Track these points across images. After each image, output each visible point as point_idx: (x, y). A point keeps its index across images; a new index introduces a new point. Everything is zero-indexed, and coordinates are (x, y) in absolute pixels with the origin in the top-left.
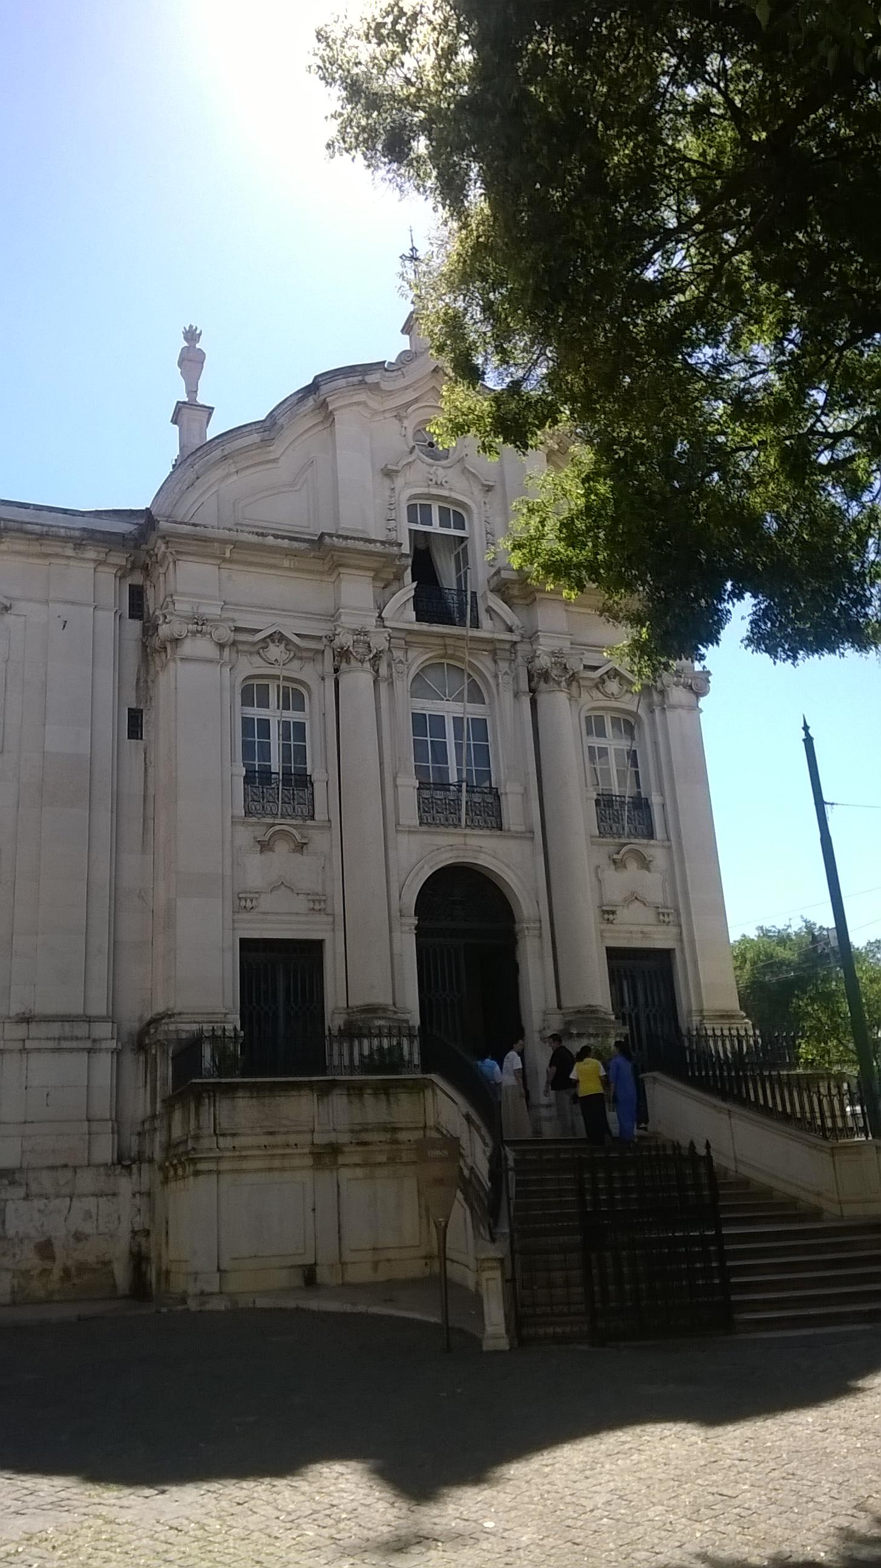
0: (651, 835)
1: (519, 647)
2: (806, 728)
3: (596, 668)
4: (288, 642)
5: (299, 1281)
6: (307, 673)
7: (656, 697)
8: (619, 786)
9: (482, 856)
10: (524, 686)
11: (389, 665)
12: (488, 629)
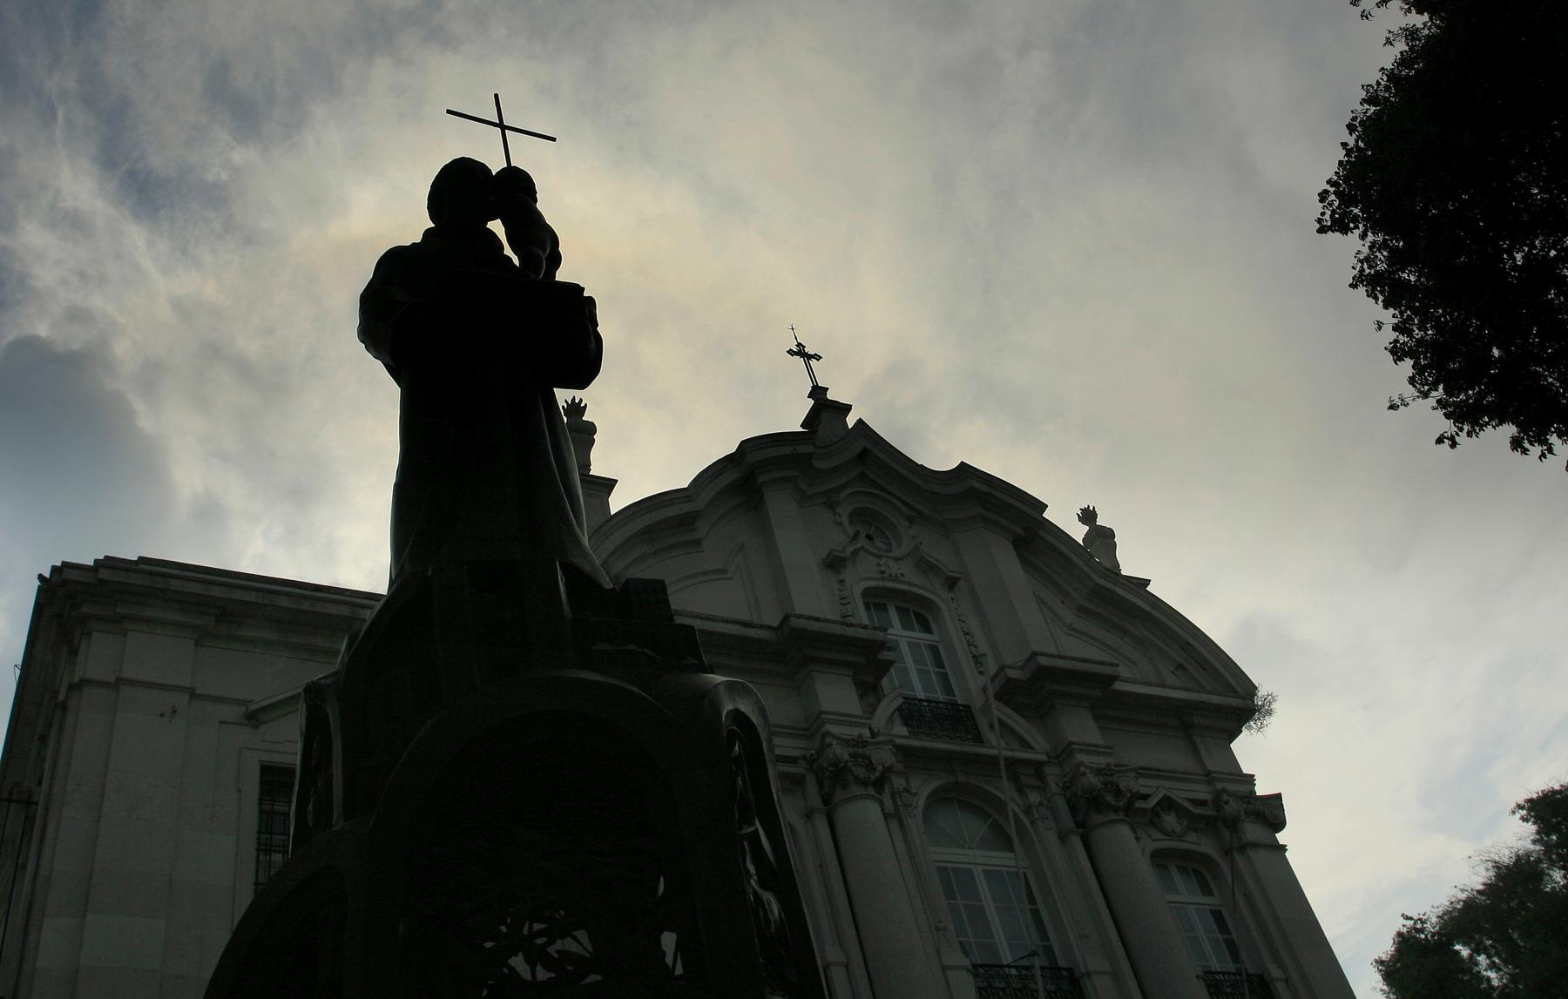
1: (1047, 770)
3: (1145, 797)
10: (1068, 822)
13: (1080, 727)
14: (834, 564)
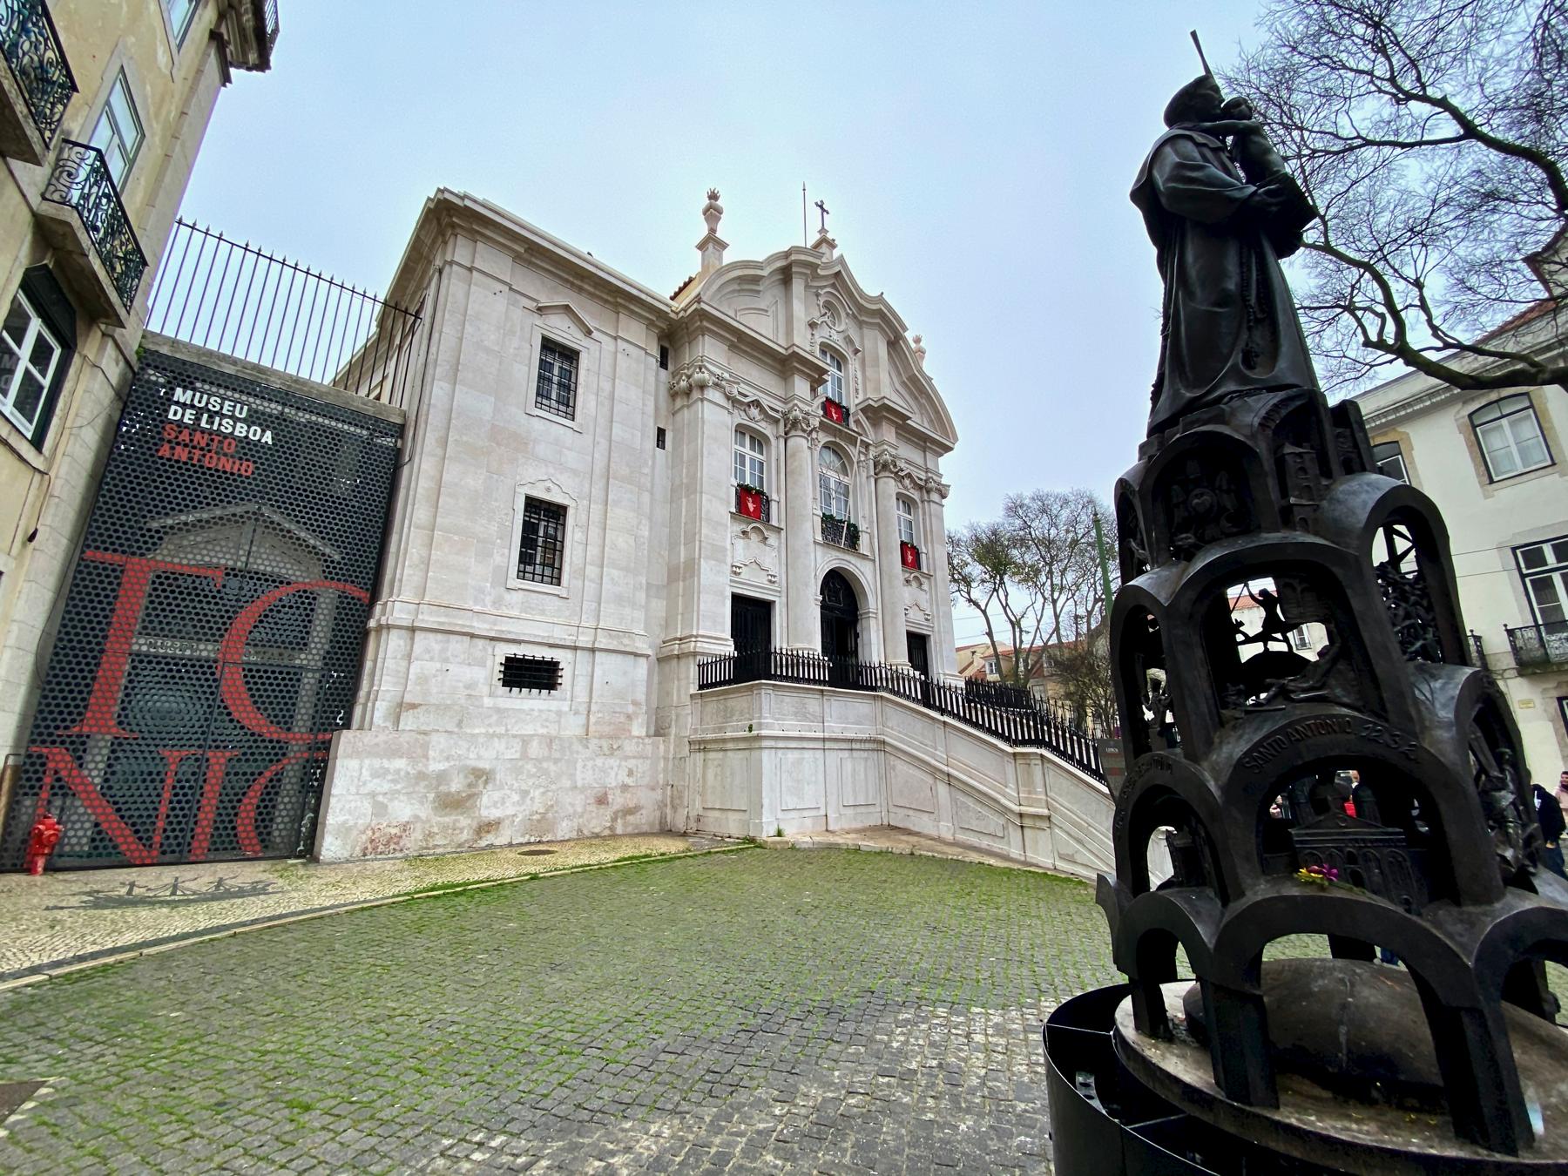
13: (889, 434)
14: (813, 325)
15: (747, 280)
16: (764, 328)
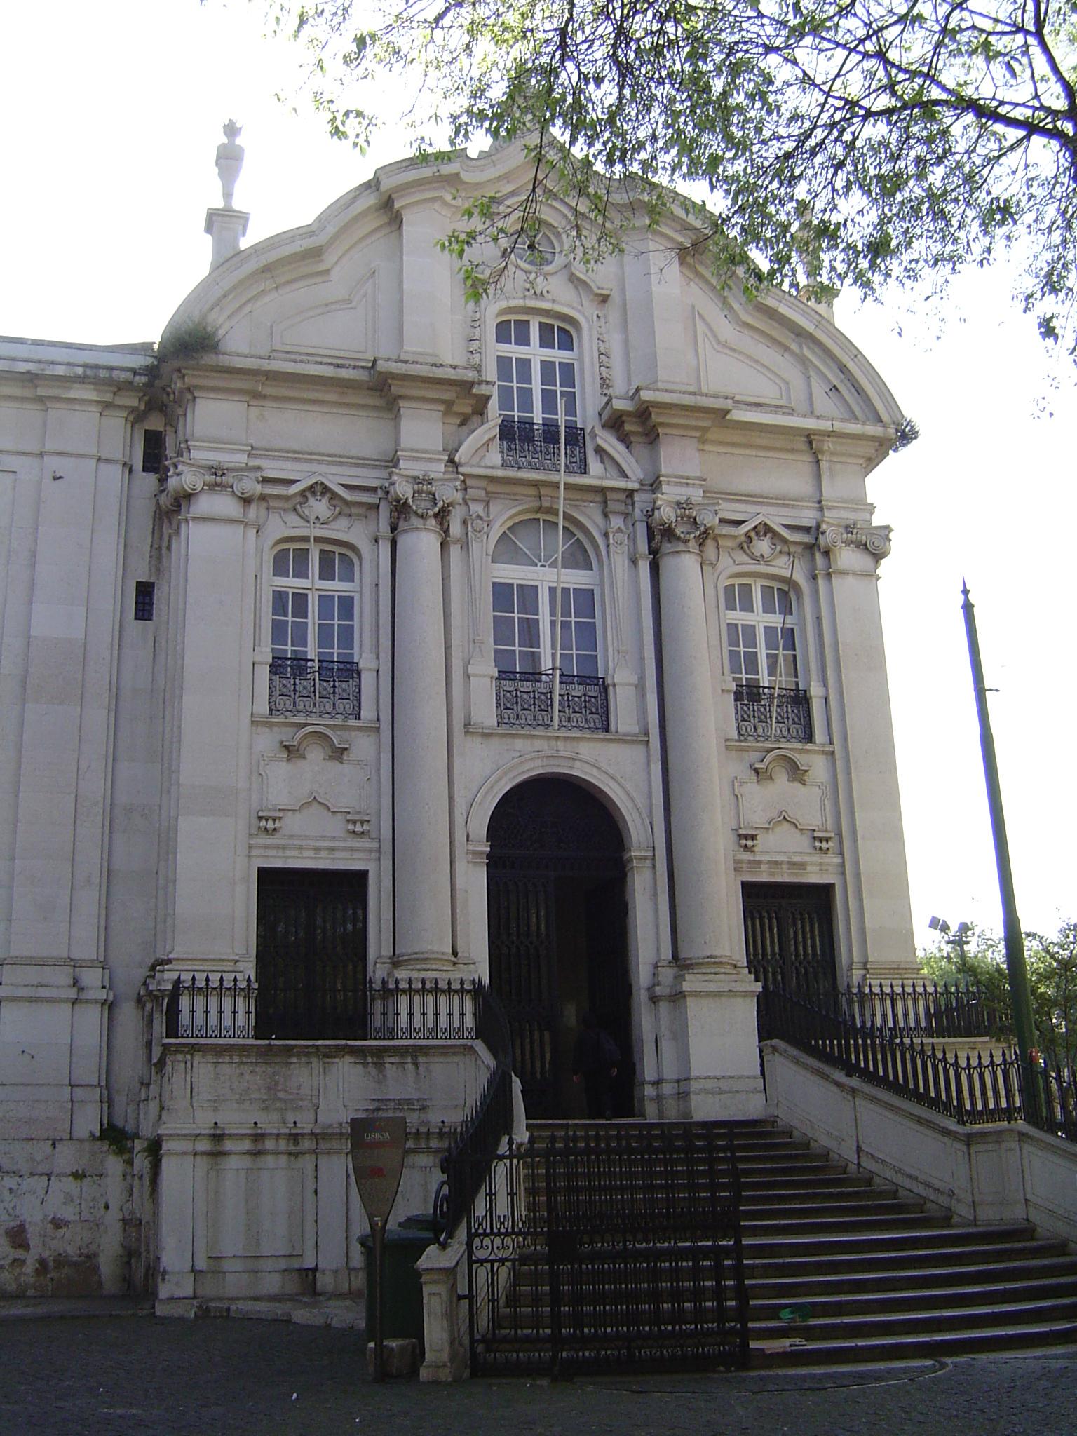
0: (809, 738)
1: (637, 497)
2: (965, 592)
3: (739, 523)
4: (334, 496)
5: (292, 1287)
6: (355, 533)
7: (819, 559)
8: (770, 675)
9: (578, 764)
10: (643, 547)
11: (465, 522)
12: (596, 473)
15: (297, 258)
16: (334, 333)
